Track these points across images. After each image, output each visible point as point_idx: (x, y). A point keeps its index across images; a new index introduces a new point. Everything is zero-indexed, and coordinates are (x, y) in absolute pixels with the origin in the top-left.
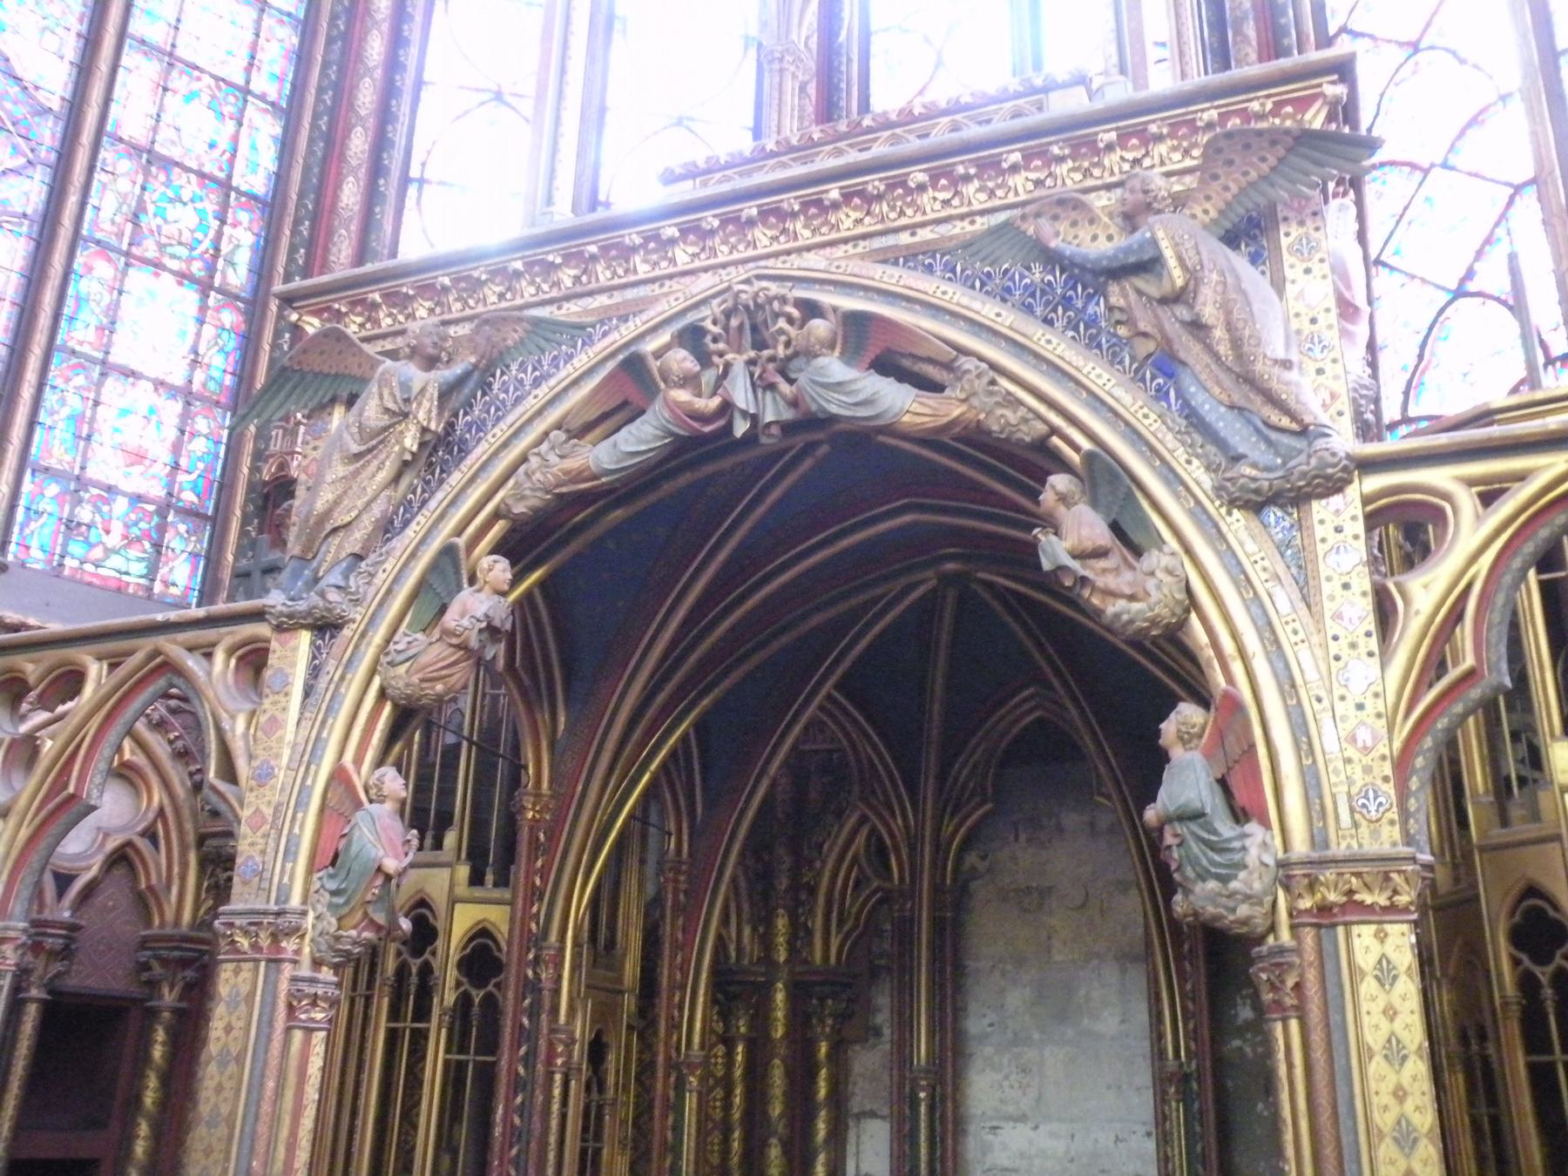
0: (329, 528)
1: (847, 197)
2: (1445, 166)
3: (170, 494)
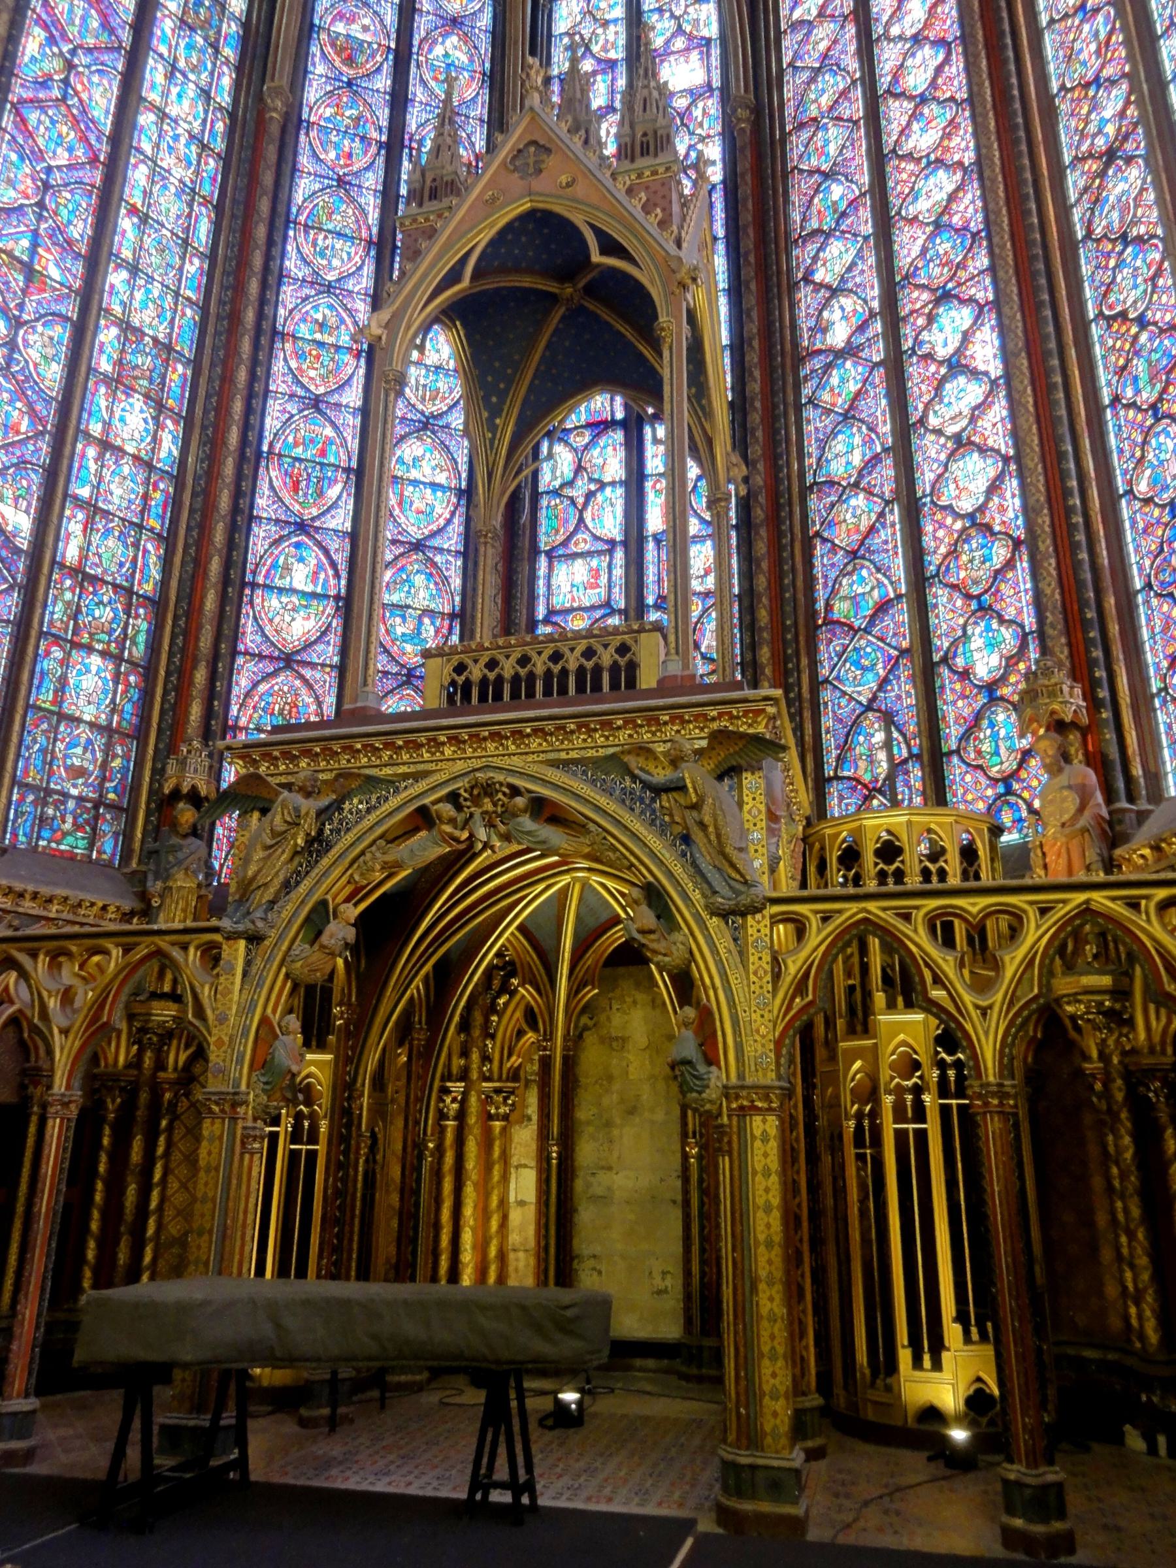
0: (254, 886)
1: (535, 731)
2: (865, 630)
3: (101, 796)
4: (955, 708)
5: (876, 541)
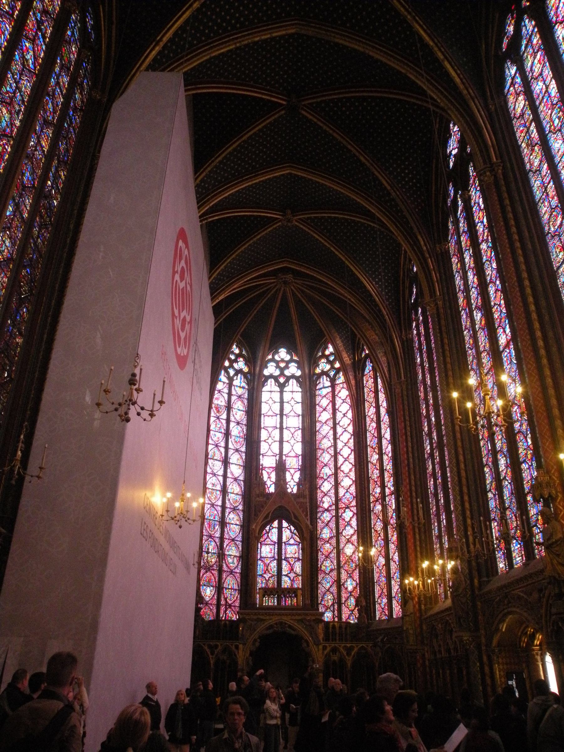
4: (344, 595)
5: (331, 555)
